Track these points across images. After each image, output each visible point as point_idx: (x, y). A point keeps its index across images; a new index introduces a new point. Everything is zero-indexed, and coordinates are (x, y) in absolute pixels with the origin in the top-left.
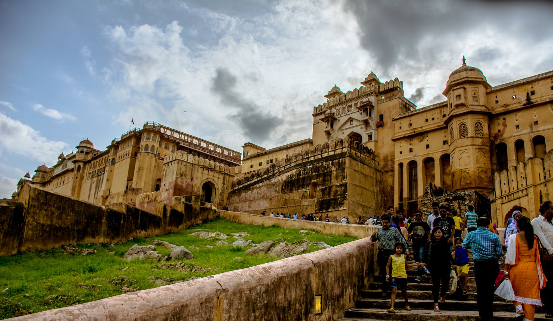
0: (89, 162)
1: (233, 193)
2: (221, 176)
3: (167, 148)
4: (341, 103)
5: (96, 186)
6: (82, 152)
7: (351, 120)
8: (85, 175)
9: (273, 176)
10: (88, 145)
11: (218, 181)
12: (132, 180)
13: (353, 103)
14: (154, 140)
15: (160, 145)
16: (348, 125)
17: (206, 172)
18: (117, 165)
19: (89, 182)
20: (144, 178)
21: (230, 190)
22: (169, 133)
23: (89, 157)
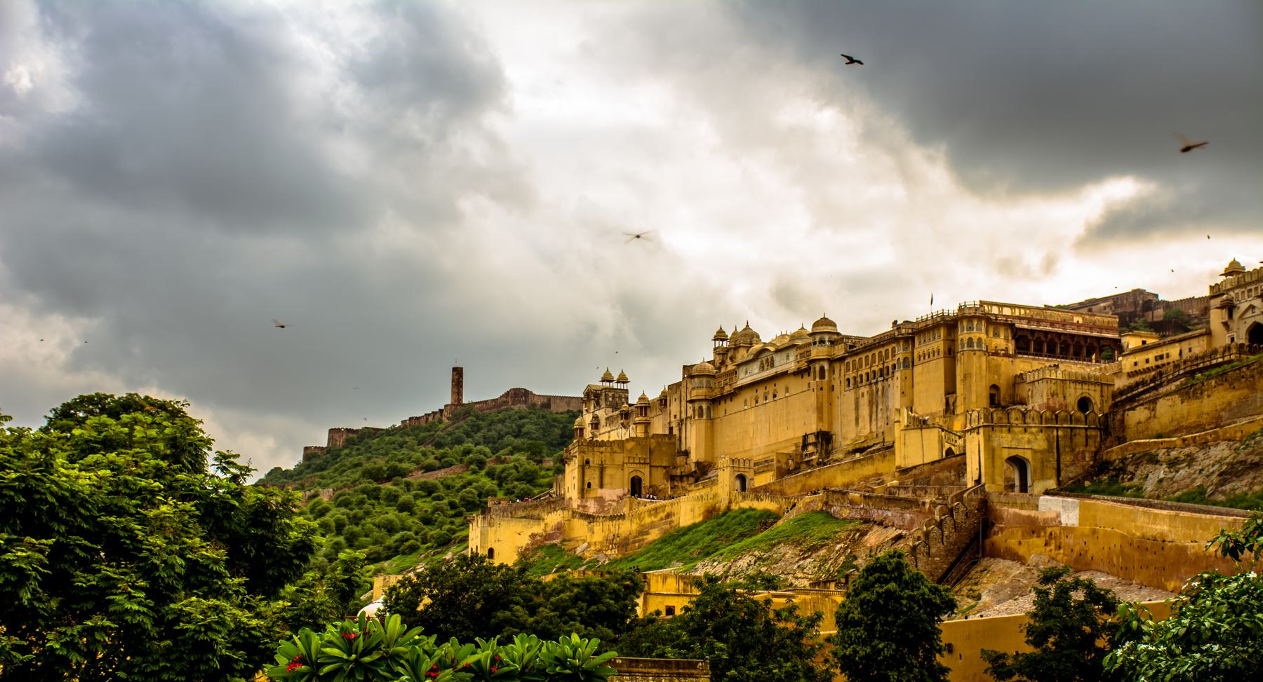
0: (842, 359)
1: (1115, 405)
2: (1098, 388)
3: (996, 335)
4: (1239, 286)
5: (871, 402)
6: (822, 342)
7: (1252, 307)
8: (836, 383)
9: (1161, 385)
10: (830, 329)
11: (1095, 394)
12: (954, 392)
13: (1253, 287)
14: (979, 330)
15: (987, 333)
16: (1249, 314)
17: (1079, 386)
18: (917, 369)
19: (850, 396)
20: (974, 388)
21: (1110, 402)
22: (995, 310)
23: (839, 351)
